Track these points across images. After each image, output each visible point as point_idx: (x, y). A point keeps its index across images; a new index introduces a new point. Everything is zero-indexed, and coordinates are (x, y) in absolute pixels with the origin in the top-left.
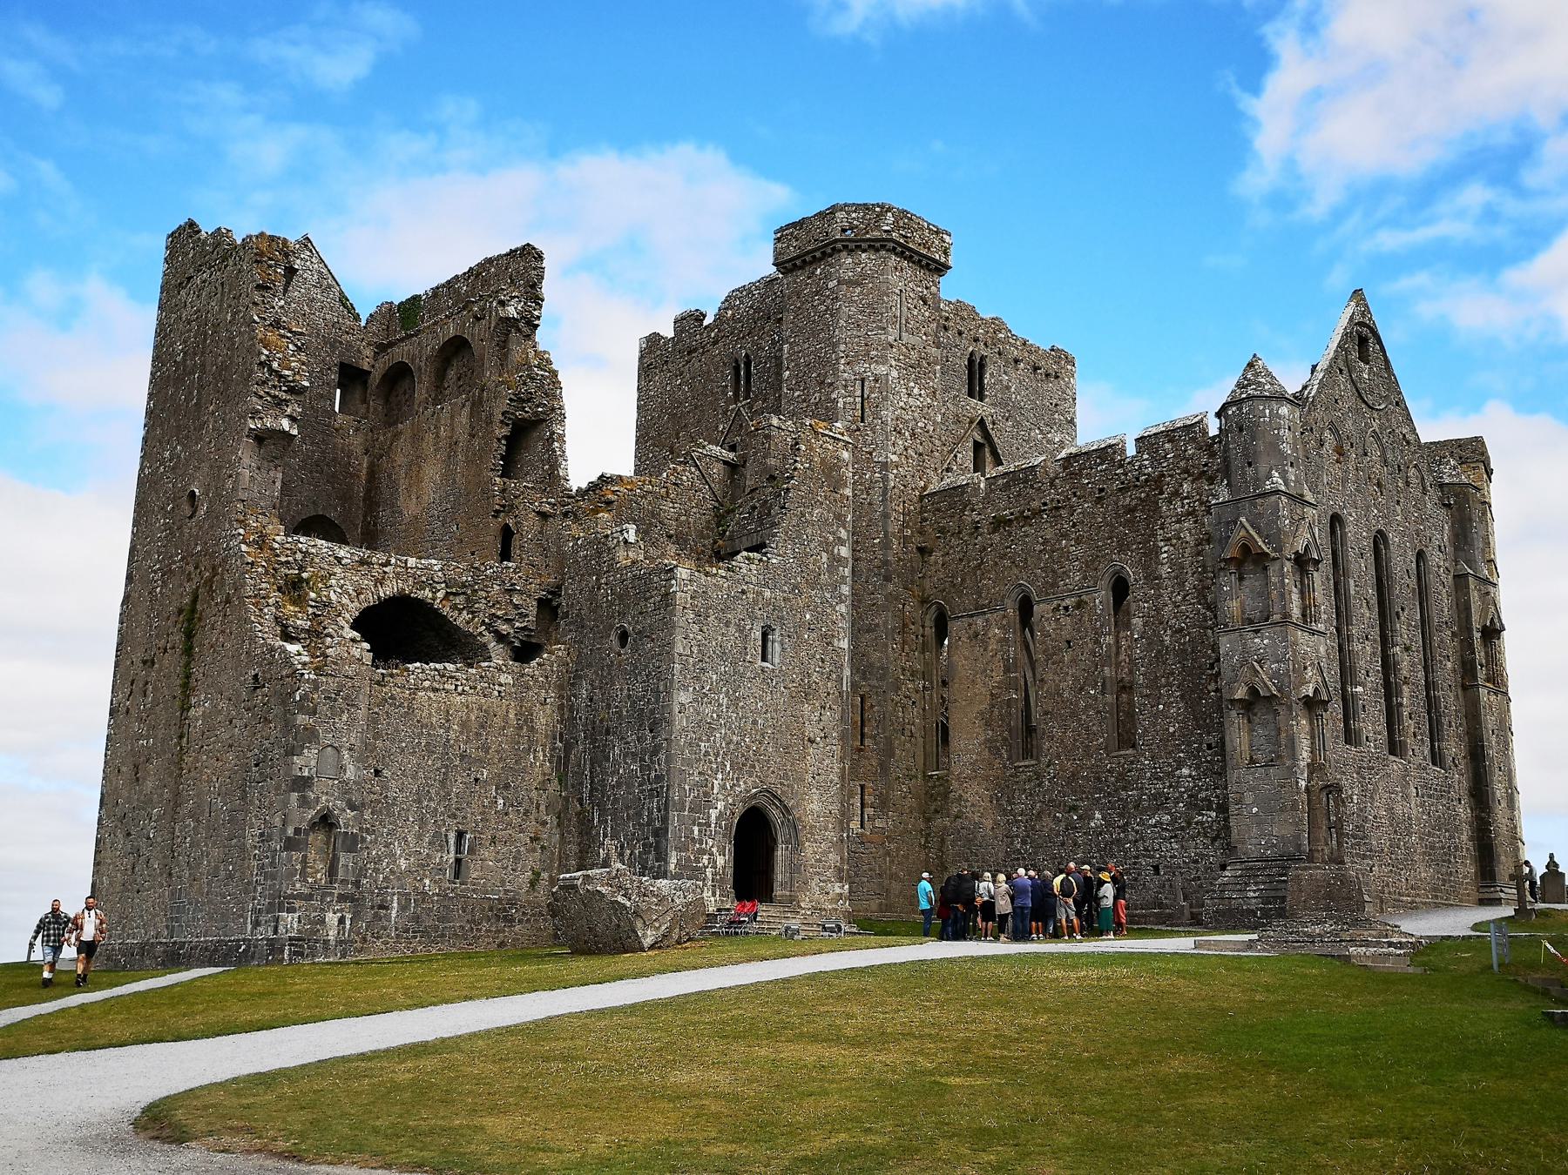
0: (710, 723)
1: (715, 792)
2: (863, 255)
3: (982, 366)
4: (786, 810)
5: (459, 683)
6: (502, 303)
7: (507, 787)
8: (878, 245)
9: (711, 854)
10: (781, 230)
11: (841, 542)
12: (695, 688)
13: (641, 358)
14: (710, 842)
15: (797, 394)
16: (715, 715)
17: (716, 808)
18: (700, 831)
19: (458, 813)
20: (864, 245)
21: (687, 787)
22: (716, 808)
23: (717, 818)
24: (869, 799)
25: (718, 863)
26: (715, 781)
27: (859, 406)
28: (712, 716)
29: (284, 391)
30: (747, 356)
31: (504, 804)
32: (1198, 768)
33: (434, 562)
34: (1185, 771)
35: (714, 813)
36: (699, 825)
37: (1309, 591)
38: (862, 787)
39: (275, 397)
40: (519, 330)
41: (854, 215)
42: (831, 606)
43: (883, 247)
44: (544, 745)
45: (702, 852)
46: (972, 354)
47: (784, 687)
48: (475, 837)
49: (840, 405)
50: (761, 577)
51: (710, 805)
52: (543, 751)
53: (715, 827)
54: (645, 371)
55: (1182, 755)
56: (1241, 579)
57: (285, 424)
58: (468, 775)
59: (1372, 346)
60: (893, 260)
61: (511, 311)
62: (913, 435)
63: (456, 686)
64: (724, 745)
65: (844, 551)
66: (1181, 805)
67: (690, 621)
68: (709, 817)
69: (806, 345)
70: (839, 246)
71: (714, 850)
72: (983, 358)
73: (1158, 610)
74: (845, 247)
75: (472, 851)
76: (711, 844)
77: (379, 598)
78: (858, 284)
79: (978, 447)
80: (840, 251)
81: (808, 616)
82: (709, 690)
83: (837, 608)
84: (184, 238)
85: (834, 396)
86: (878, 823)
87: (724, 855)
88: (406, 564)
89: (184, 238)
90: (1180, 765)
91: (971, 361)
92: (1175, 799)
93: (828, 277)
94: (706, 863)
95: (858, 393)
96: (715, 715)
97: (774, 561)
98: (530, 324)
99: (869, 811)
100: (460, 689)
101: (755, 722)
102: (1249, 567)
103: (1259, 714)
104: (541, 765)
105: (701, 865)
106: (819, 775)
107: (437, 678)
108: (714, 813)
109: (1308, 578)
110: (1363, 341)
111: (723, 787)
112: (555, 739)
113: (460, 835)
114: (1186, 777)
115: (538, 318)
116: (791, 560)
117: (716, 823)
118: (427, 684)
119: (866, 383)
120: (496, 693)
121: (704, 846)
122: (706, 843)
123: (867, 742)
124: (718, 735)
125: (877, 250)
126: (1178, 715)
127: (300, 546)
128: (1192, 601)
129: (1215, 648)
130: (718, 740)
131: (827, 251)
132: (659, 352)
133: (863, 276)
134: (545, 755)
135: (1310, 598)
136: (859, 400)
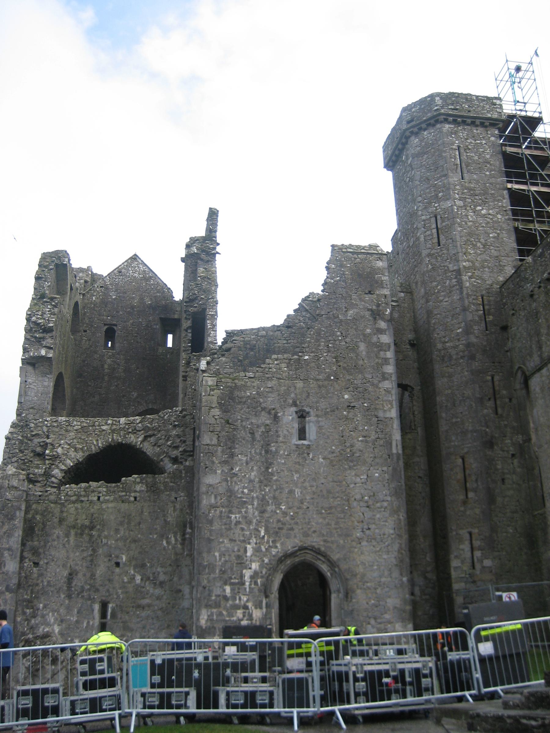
0: (241, 498)
1: (249, 554)
2: (425, 133)
4: (332, 564)
5: (101, 495)
7: (143, 566)
9: (246, 607)
11: (380, 331)
12: (223, 471)
14: (245, 598)
16: (246, 491)
17: (250, 568)
18: (232, 590)
19: (101, 588)
20: (424, 126)
21: (217, 554)
22: (250, 568)
23: (252, 577)
24: (477, 543)
25: (254, 615)
26: (248, 546)
27: (435, 235)
28: (243, 492)
29: (41, 333)
31: (142, 579)
33: (137, 417)
35: (247, 574)
36: (232, 584)
38: (470, 534)
39: (36, 337)
40: (202, 260)
41: (413, 110)
42: (373, 385)
43: (437, 122)
44: (175, 534)
45: (237, 607)
47: (323, 459)
48: (117, 606)
50: (291, 373)
51: (241, 563)
52: (175, 537)
53: (250, 585)
57: (43, 352)
58: (109, 560)
60: (447, 127)
62: (484, 246)
63: (99, 498)
64: (256, 513)
65: (386, 339)
67: (216, 417)
68: (242, 576)
70: (408, 133)
71: (250, 605)
74: (412, 133)
75: (113, 615)
76: (245, 599)
77: (99, 447)
80: (410, 137)
81: (346, 397)
82: (240, 470)
83: (380, 385)
86: (487, 563)
87: (261, 608)
88: (119, 421)
94: (241, 616)
95: (434, 226)
96: (246, 491)
97: (306, 357)
99: (478, 554)
100: (101, 499)
101: (291, 492)
104: (174, 548)
105: (235, 618)
106: (369, 529)
107: (83, 493)
108: (247, 574)
111: (257, 550)
112: (185, 526)
113: (104, 606)
116: (325, 354)
117: (251, 582)
118: (74, 498)
119: (438, 217)
120: (132, 499)
121: (237, 602)
122: (240, 599)
123: (471, 495)
124: (250, 507)
125: (434, 125)
127: (46, 423)
130: (251, 511)
134: (176, 540)
136: (435, 231)
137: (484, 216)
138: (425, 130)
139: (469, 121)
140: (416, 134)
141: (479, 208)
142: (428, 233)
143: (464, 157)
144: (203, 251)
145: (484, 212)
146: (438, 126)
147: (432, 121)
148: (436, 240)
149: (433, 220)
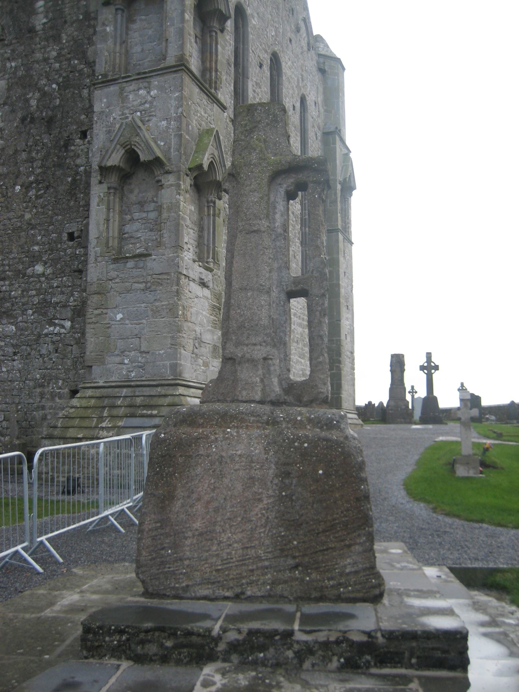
32: (55, 262)
34: (39, 268)
37: (211, 53)
55: (36, 248)
56: (130, 20)
66: (30, 312)
73: (28, 69)
90: (35, 259)
92: (23, 305)
103: (136, 191)
109: (211, 36)
114: (39, 276)
126: (38, 197)
128: (69, 56)
129: (89, 110)
135: (211, 61)
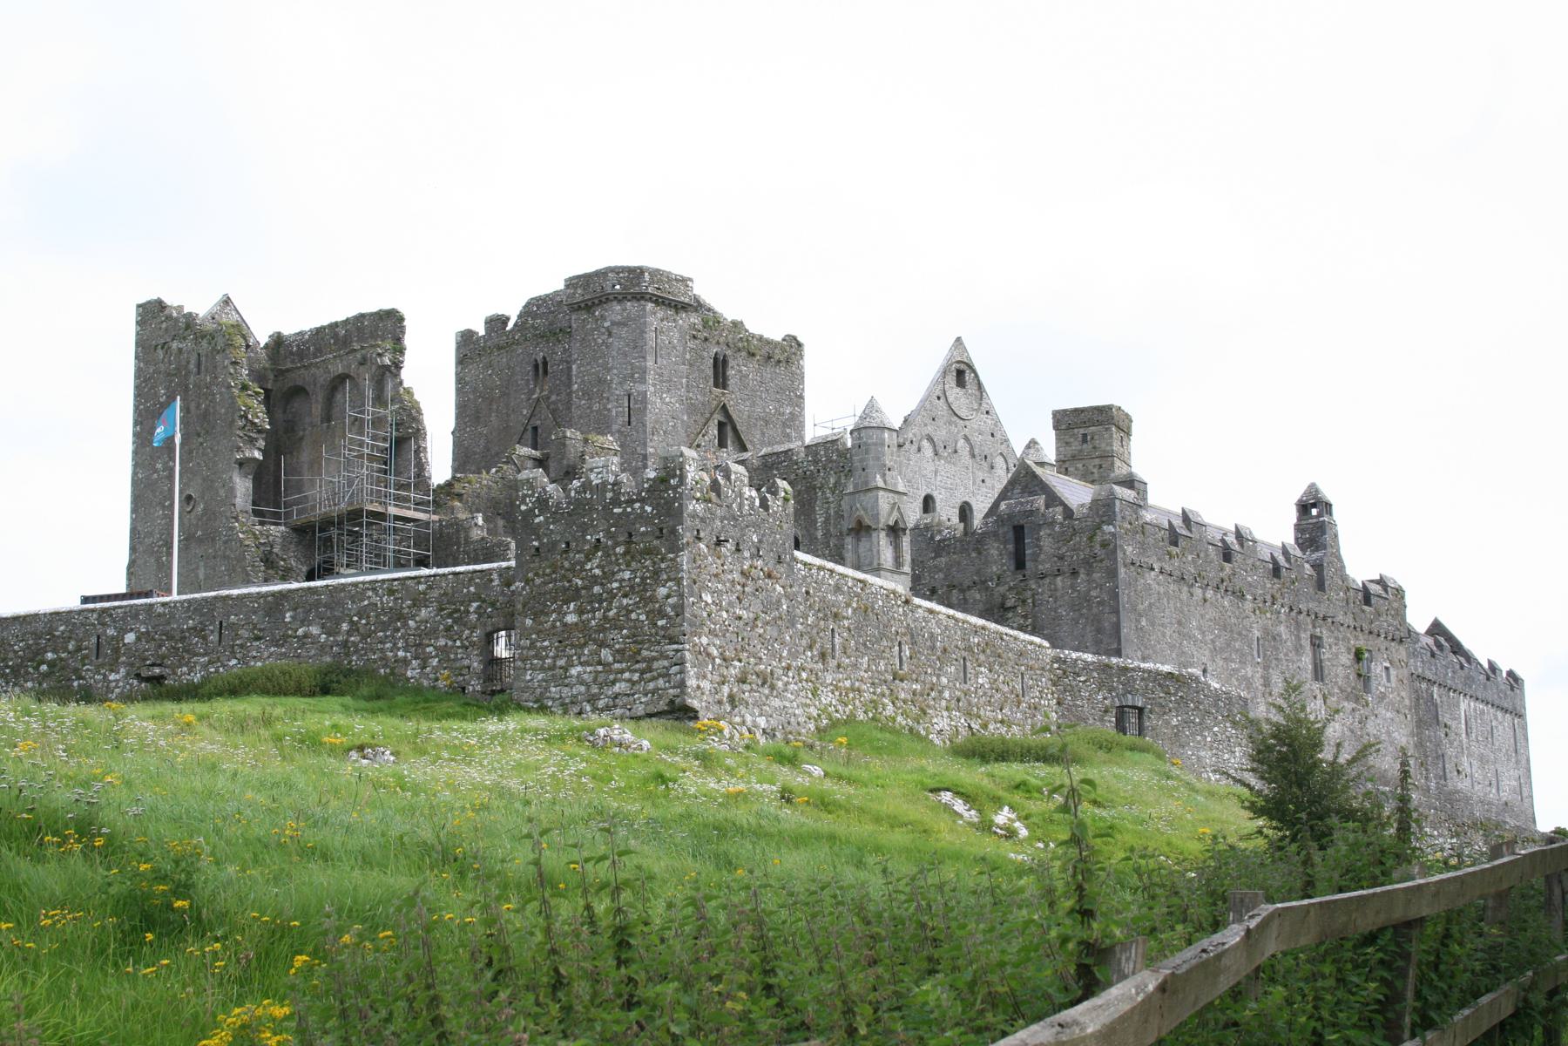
2: (629, 304)
3: (725, 362)
6: (380, 355)
8: (639, 296)
10: (571, 279)
13: (458, 349)
15: (583, 402)
20: (629, 297)
27: (627, 414)
30: (544, 358)
40: (390, 372)
41: (621, 275)
43: (642, 298)
46: (716, 354)
49: (614, 413)
54: (462, 361)
56: (859, 540)
59: (969, 377)
60: (650, 306)
61: (387, 361)
62: (665, 432)
69: (589, 367)
72: (725, 356)
78: (625, 325)
79: (721, 425)
84: (152, 315)
85: (609, 406)
89: (152, 315)
91: (716, 359)
93: (603, 318)
95: (627, 405)
98: (398, 366)
102: (863, 533)
110: (960, 374)
115: (402, 362)
119: (632, 398)
125: (638, 300)
131: (604, 299)
132: (472, 346)
133: (629, 318)
136: (627, 409)
137: (667, 404)
138: (629, 301)
139: (667, 302)
140: (619, 301)
141: (665, 395)
142: (621, 409)
143: (659, 341)
144: (394, 363)
145: (667, 400)
146: (642, 302)
147: (639, 296)
148: (627, 419)
149: (626, 398)
